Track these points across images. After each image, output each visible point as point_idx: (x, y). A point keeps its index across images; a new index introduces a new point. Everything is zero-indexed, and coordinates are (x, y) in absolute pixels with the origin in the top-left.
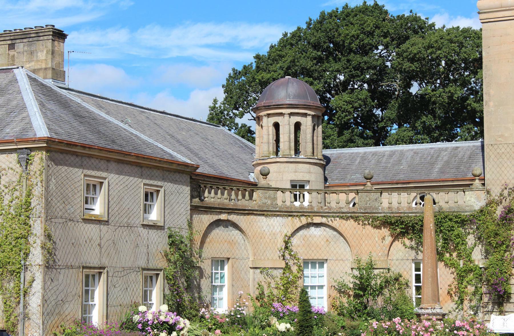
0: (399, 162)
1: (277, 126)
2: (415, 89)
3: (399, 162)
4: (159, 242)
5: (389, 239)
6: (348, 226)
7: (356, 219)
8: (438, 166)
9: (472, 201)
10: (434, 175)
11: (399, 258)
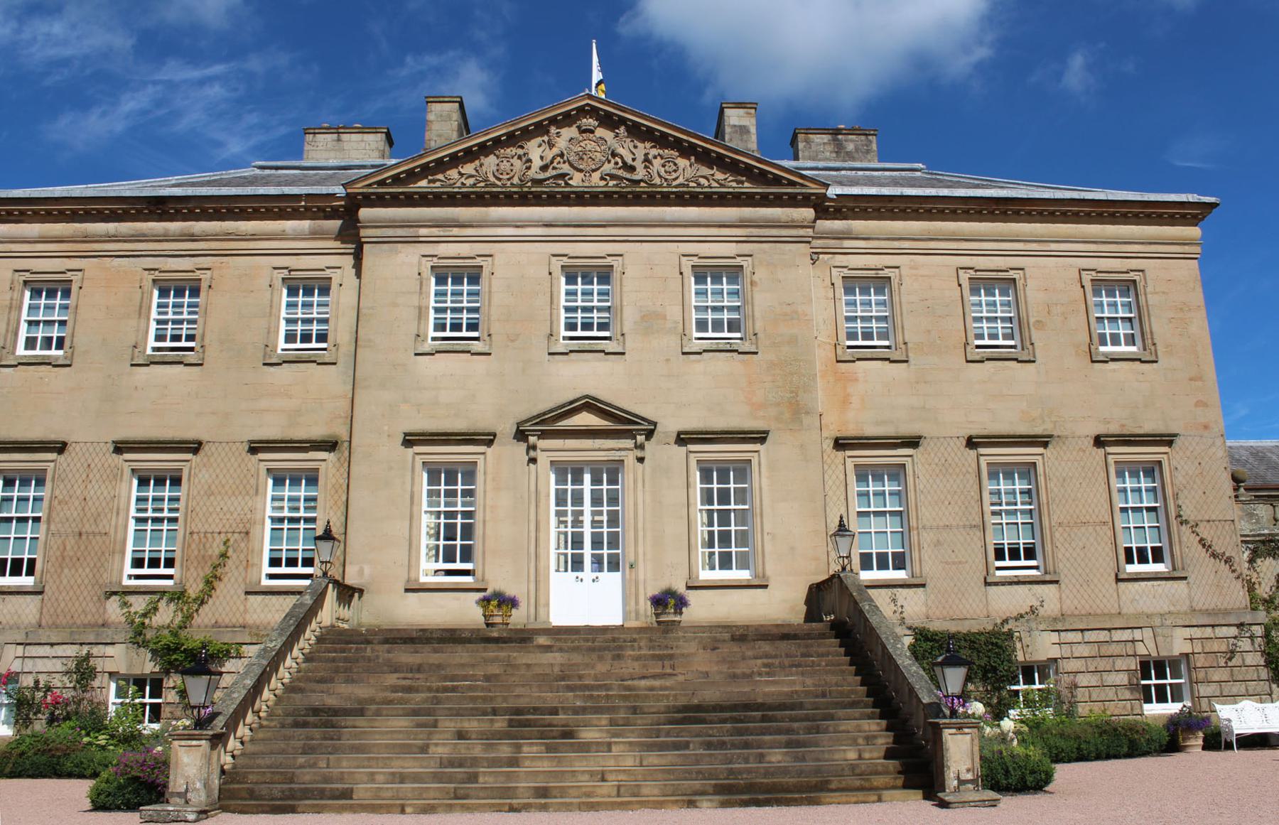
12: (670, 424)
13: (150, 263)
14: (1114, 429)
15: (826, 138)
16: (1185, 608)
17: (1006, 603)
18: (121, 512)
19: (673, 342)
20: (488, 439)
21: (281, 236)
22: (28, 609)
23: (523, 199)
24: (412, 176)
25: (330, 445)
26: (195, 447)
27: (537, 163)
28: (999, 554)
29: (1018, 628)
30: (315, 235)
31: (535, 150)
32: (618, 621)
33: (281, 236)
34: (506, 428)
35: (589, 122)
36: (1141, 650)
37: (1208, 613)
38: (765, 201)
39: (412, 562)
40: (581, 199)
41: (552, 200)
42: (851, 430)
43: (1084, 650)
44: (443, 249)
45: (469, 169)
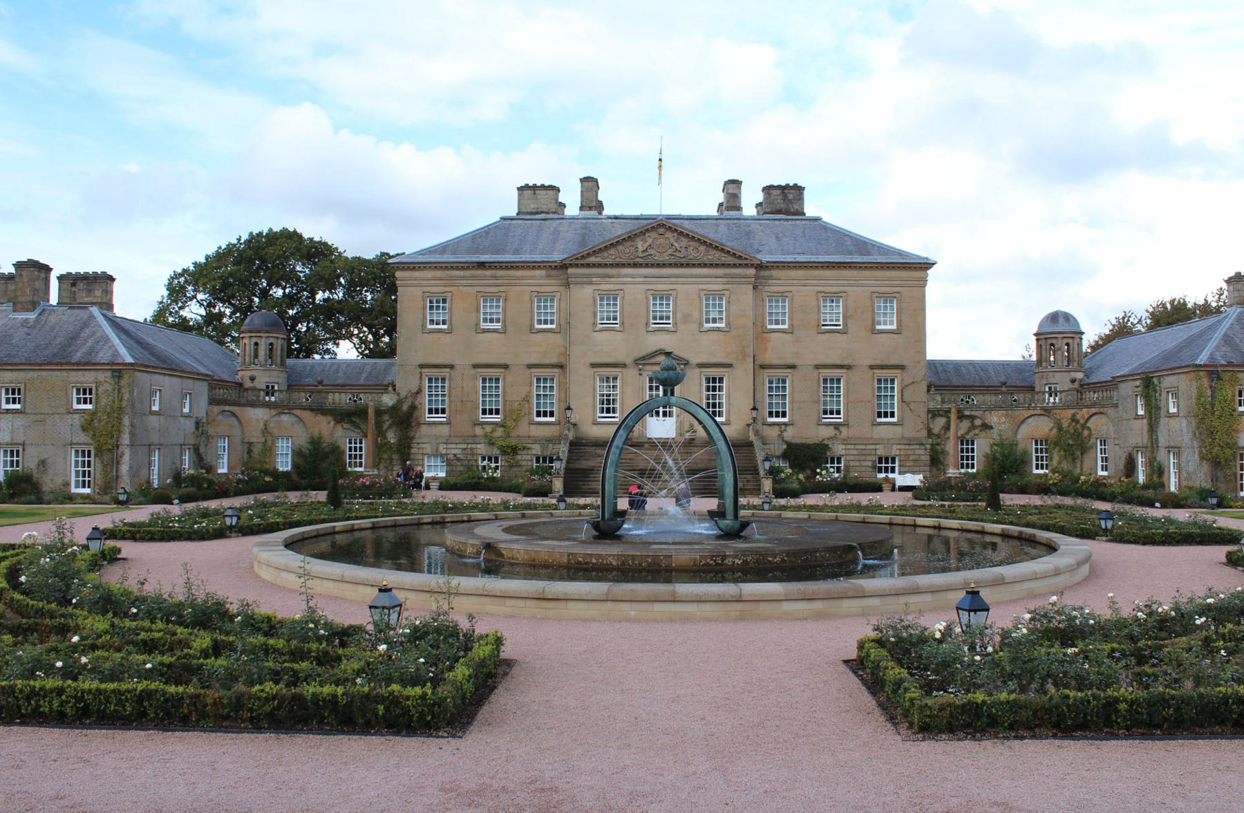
0: (337, 371)
1: (256, 344)
2: (320, 296)
3: (337, 371)
4: (189, 425)
5: (332, 423)
6: (306, 415)
7: (312, 410)
8: (364, 376)
9: (388, 400)
10: (362, 381)
11: (342, 436)
12: (694, 360)
13: (479, 289)
14: (878, 362)
15: (779, 192)
16: (899, 436)
17: (825, 433)
18: (477, 392)
19: (696, 326)
20: (624, 366)
21: (533, 277)
22: (445, 430)
23: (635, 265)
26: (506, 367)
27: (641, 248)
28: (825, 412)
29: (829, 443)
30: (548, 276)
31: (641, 246)
33: (533, 277)
34: (629, 361)
35: (661, 230)
36: (879, 453)
37: (909, 439)
38: (735, 266)
39: (594, 415)
40: (658, 266)
41: (647, 266)
42: (767, 362)
43: (855, 452)
44: (601, 287)
45: (612, 251)
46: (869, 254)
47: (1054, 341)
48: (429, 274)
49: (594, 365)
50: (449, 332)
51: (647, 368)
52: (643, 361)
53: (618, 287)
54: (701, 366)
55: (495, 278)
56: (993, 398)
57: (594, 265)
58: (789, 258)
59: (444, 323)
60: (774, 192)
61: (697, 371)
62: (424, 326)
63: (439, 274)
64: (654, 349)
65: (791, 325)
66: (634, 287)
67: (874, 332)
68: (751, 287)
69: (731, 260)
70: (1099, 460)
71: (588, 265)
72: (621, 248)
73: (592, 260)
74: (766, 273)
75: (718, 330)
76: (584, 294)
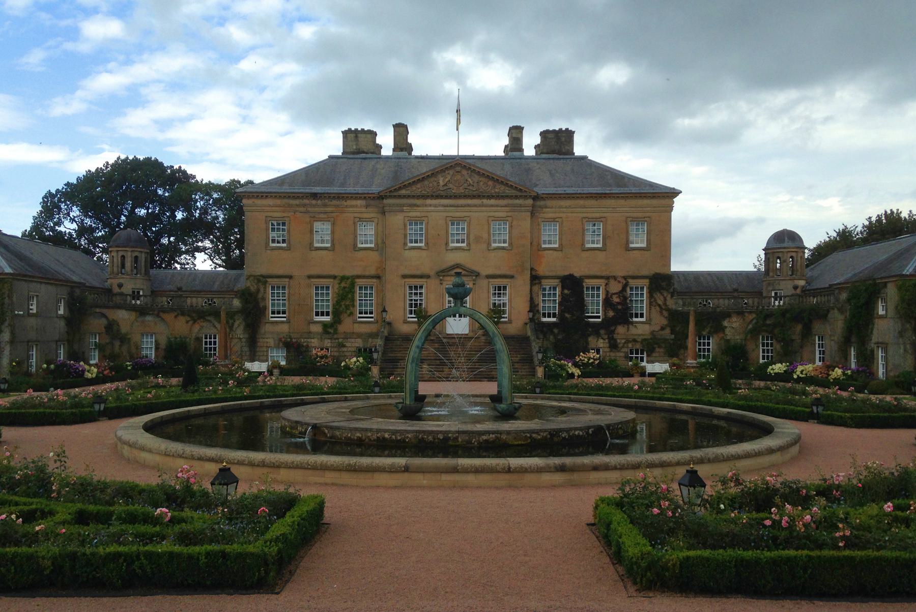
0: (194, 280)
1: (123, 257)
3: (194, 280)
12: (484, 273)
14: (630, 273)
18: (311, 298)
19: (484, 246)
20: (428, 277)
24: (400, 188)
25: (378, 277)
27: (441, 183)
32: (467, 332)
33: (356, 206)
34: (432, 273)
35: (458, 169)
38: (516, 197)
40: (456, 197)
41: (447, 197)
45: (419, 186)
46: (625, 186)
47: (780, 255)
48: (270, 202)
49: (404, 276)
50: (288, 249)
51: (448, 278)
52: (442, 273)
53: (423, 214)
54: (489, 277)
55: (325, 205)
56: (726, 301)
57: (404, 197)
58: (560, 190)
59: (284, 241)
60: (550, 136)
61: (486, 281)
62: (267, 244)
63: (278, 202)
64: (453, 263)
65: (561, 245)
66: (436, 212)
67: (628, 249)
68: (529, 214)
69: (514, 192)
70: (817, 353)
71: (400, 197)
72: (426, 182)
73: (403, 192)
74: (542, 203)
75: (503, 248)
76: (396, 220)
